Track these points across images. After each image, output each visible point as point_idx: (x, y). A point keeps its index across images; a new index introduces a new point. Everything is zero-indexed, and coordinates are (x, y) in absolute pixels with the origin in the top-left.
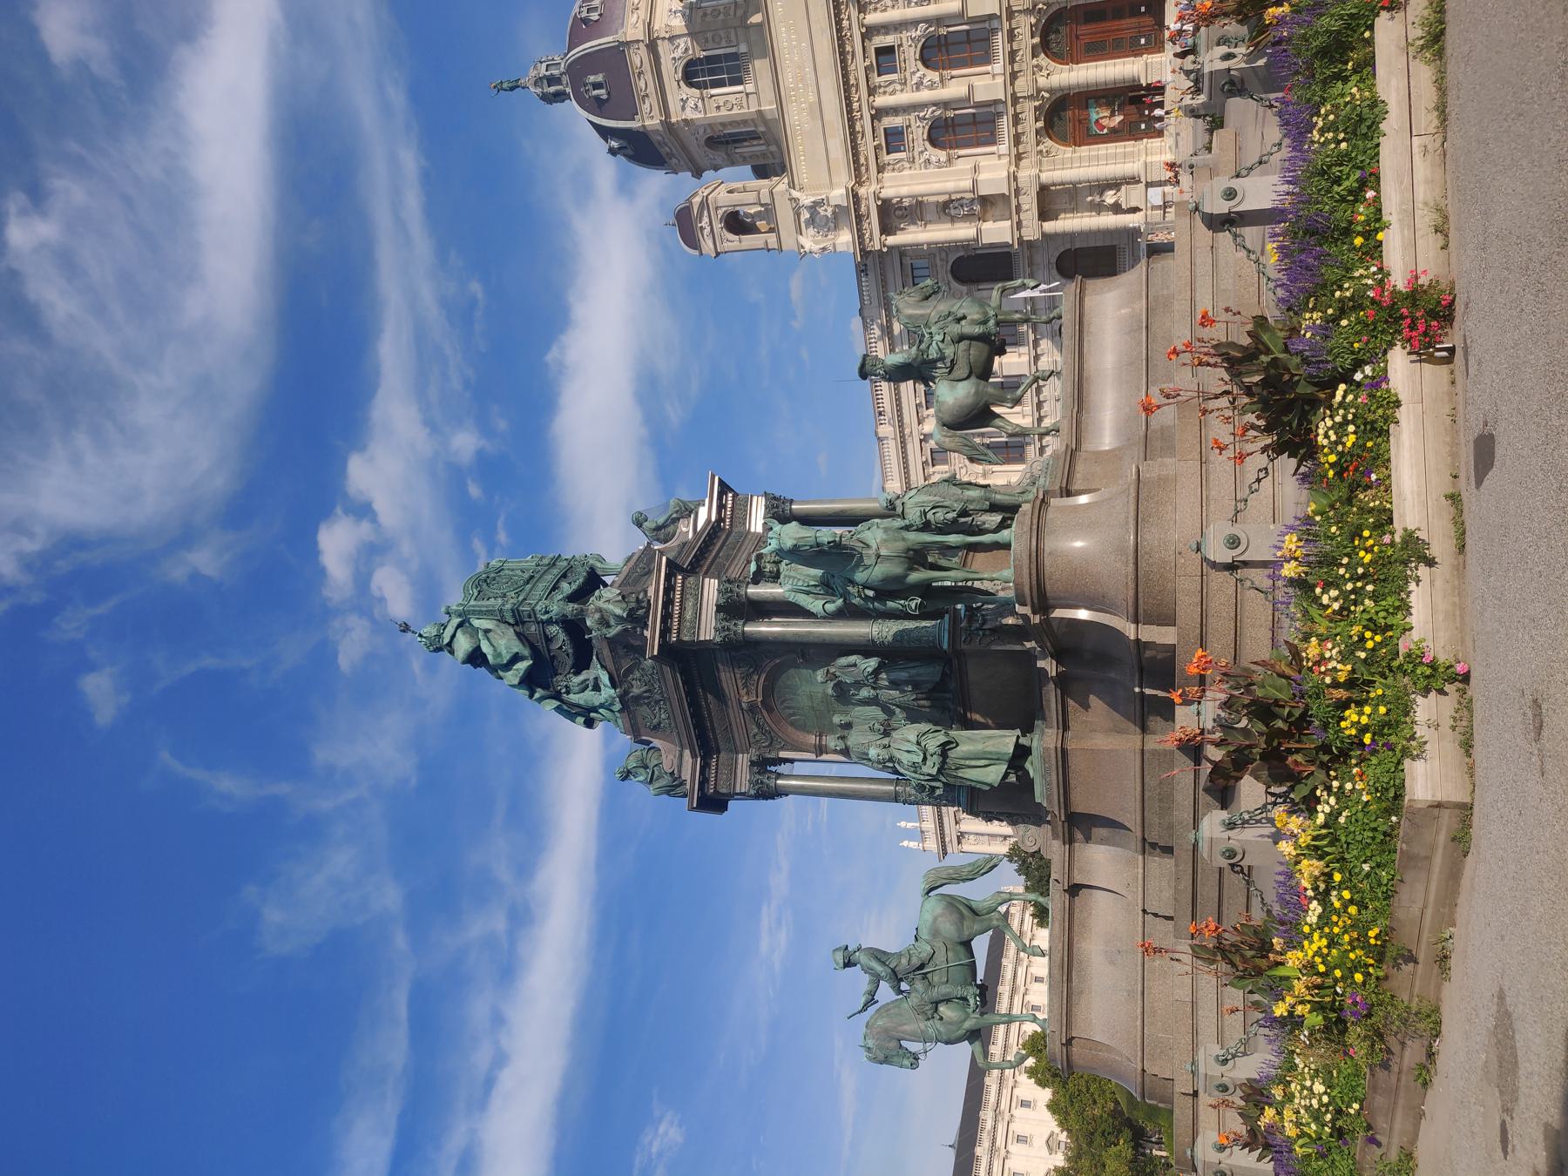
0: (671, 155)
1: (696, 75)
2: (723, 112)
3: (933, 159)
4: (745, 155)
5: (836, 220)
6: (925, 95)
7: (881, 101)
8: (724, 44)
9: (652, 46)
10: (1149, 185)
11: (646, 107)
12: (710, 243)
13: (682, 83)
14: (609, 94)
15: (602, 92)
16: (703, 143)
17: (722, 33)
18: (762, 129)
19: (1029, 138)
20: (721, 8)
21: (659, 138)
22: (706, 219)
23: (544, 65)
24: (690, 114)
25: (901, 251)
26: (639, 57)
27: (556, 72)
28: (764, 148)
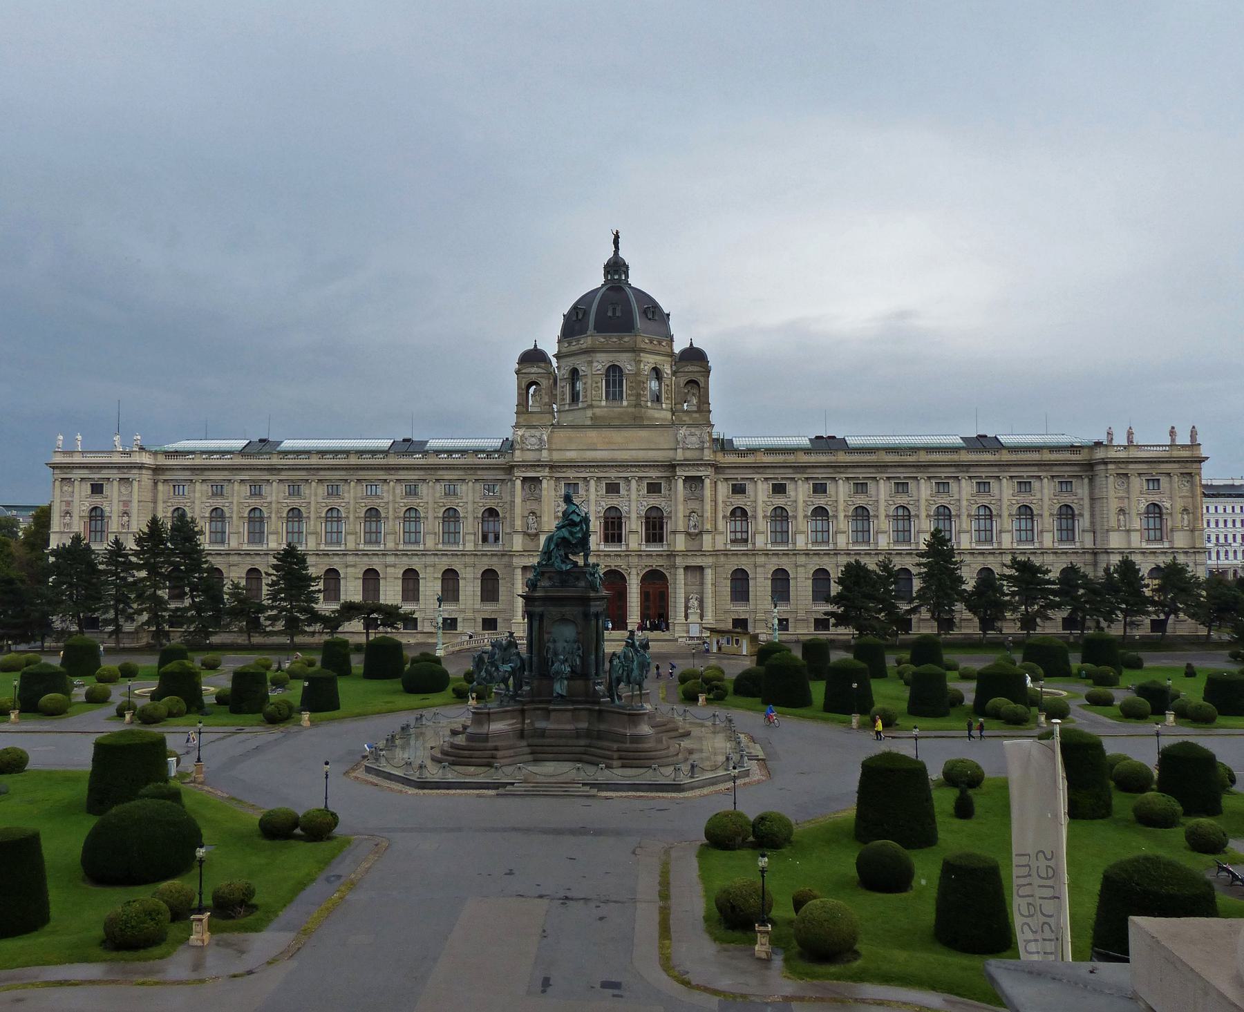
0: (570, 344)
1: (614, 372)
3: (560, 509)
4: (565, 388)
7: (592, 483)
8: (629, 392)
13: (611, 364)
14: (610, 317)
15: (610, 314)
18: (580, 405)
20: (645, 393)
21: (582, 342)
28: (568, 402)
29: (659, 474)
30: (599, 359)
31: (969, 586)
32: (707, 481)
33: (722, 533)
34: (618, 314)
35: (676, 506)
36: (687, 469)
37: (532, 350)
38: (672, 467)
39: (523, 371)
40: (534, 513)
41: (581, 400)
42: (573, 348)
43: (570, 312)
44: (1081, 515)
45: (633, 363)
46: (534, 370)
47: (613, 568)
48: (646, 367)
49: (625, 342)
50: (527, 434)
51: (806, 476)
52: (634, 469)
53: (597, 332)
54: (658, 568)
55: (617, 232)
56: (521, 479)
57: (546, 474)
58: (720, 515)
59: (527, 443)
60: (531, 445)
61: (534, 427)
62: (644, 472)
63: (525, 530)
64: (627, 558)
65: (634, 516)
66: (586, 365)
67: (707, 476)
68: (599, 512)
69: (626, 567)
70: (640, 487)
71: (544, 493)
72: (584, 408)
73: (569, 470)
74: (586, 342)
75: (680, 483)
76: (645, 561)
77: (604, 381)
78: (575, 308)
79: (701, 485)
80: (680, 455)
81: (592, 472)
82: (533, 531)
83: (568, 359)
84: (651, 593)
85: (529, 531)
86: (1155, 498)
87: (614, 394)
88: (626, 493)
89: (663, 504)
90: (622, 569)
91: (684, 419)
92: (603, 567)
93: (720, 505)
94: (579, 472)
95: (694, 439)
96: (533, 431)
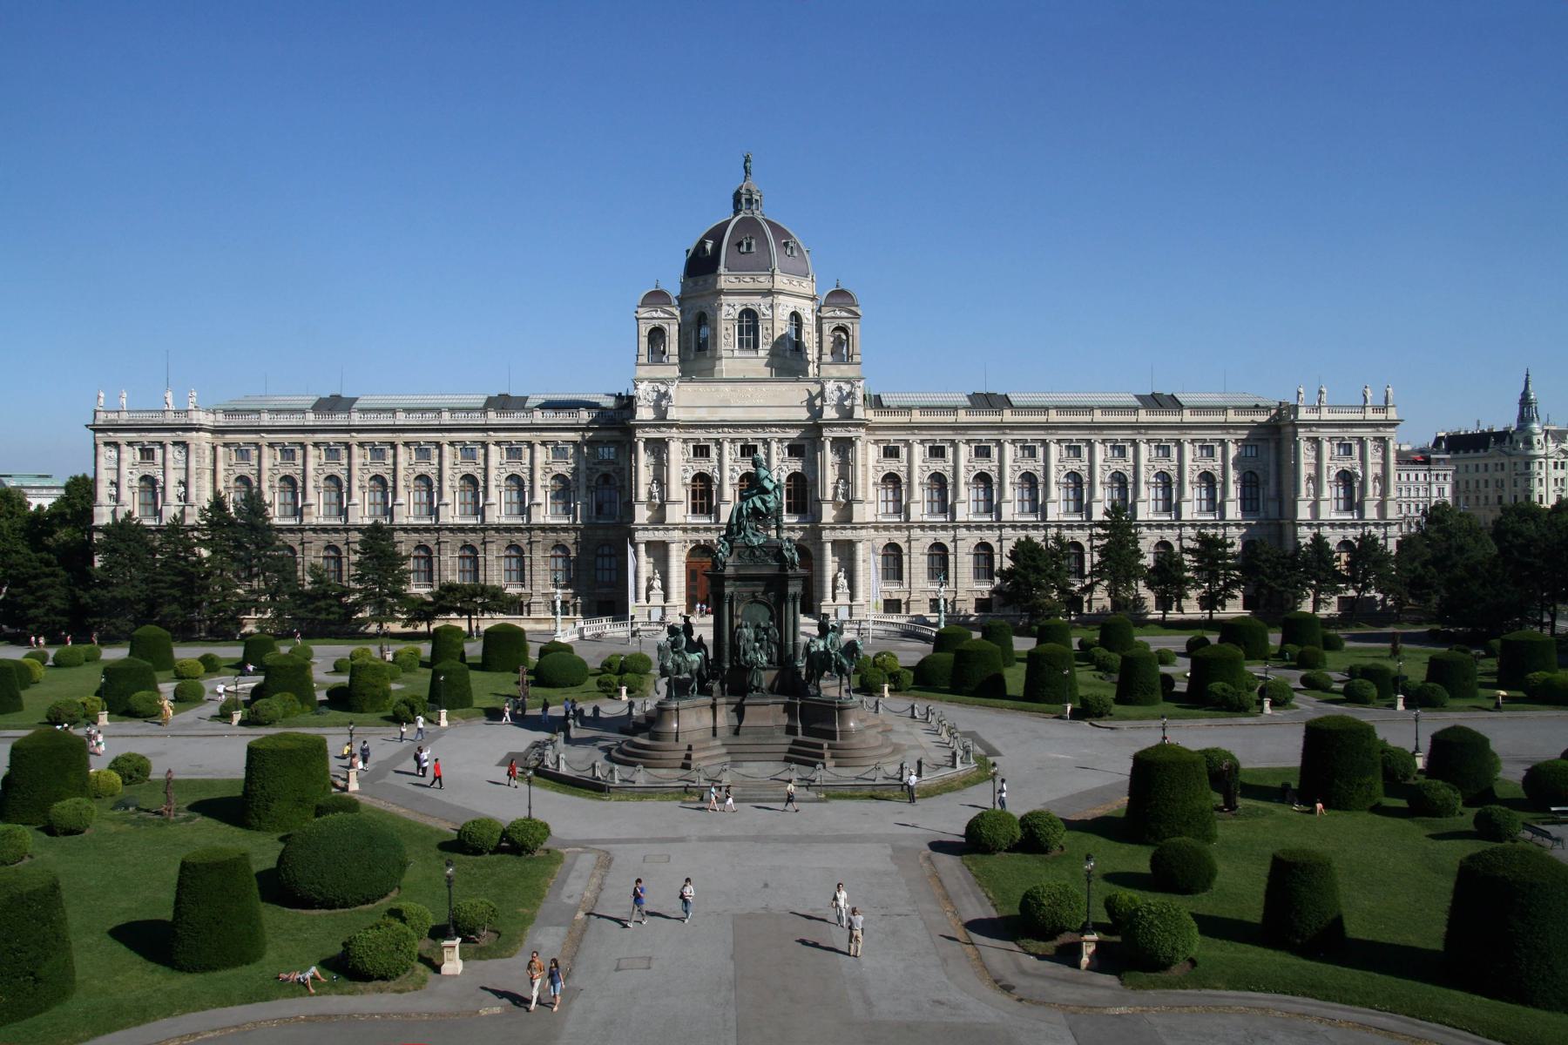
2: (724, 332)
3: (688, 475)
5: (661, 413)
6: (727, 473)
7: (726, 446)
8: (765, 340)
9: (769, 293)
10: (663, 608)
12: (645, 315)
14: (743, 253)
15: (744, 249)
19: (695, 536)
22: (662, 315)
23: (758, 198)
24: (725, 308)
25: (633, 448)
26: (764, 282)
27: (754, 206)
31: (1148, 561)
32: (859, 443)
33: (872, 503)
44: (1266, 482)
51: (967, 437)
58: (871, 481)
77: (737, 327)
86: (1346, 465)
93: (871, 471)
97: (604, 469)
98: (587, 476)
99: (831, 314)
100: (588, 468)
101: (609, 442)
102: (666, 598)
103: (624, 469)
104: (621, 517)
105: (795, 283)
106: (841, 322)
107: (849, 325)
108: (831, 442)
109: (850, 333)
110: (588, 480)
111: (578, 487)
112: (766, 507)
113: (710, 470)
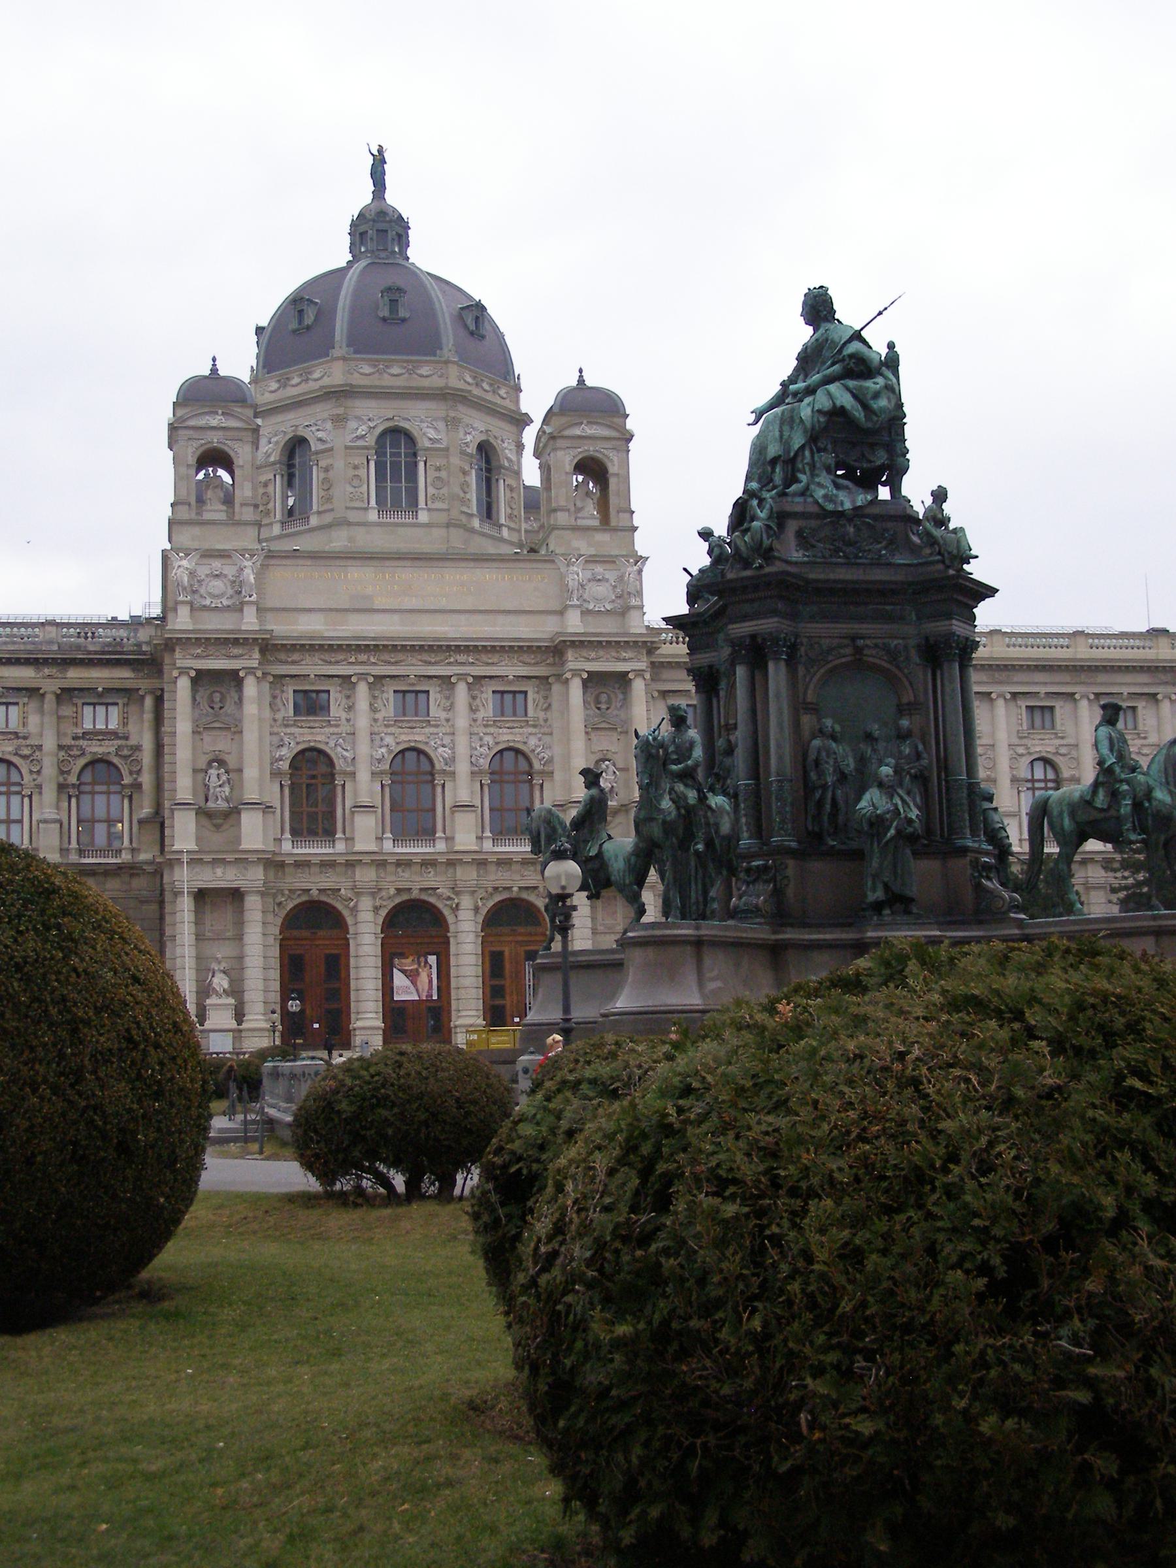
0: (284, 383)
1: (395, 445)
3: (284, 751)
4: (270, 489)
8: (431, 490)
11: (367, 369)
14: (384, 319)
16: (300, 433)
17: (444, 491)
18: (314, 521)
20: (468, 496)
21: (316, 375)
26: (428, 375)
28: (278, 517)
29: (524, 671)
30: (358, 412)
34: (402, 313)
35: (567, 740)
36: (593, 655)
37: (205, 377)
38: (556, 650)
39: (192, 423)
40: (221, 763)
41: (315, 508)
42: (291, 392)
43: (280, 317)
45: (441, 425)
46: (214, 421)
47: (415, 894)
48: (469, 438)
49: (422, 376)
50: (203, 571)
52: (461, 658)
53: (356, 352)
54: (524, 895)
55: (381, 150)
56: (193, 674)
57: (255, 664)
59: (202, 591)
60: (210, 594)
61: (223, 555)
62: (488, 664)
63: (202, 804)
64: (451, 871)
65: (463, 768)
66: (329, 425)
67: (639, 673)
68: (379, 761)
69: (447, 893)
70: (478, 700)
71: (251, 709)
72: (329, 526)
73: (308, 659)
74: (331, 373)
75: (576, 689)
76: (492, 877)
77: (372, 464)
78: (298, 303)
79: (621, 696)
80: (574, 623)
81: (362, 663)
82: (222, 805)
83: (279, 418)
84: (507, 954)
85: (211, 804)
87: (396, 492)
88: (443, 715)
89: (533, 741)
90: (439, 897)
91: (576, 544)
92: (392, 891)
94: (330, 663)
95: (601, 590)
96: (217, 564)
97: (96, 749)
98: (61, 762)
99: (577, 431)
100: (61, 747)
101: (107, 690)
102: (239, 1016)
103: (138, 748)
104: (133, 850)
105: (486, 387)
106: (590, 449)
107: (611, 454)
108: (585, 684)
109: (612, 469)
110: (62, 772)
111: (40, 787)
112: (865, 407)
113: (332, 744)
